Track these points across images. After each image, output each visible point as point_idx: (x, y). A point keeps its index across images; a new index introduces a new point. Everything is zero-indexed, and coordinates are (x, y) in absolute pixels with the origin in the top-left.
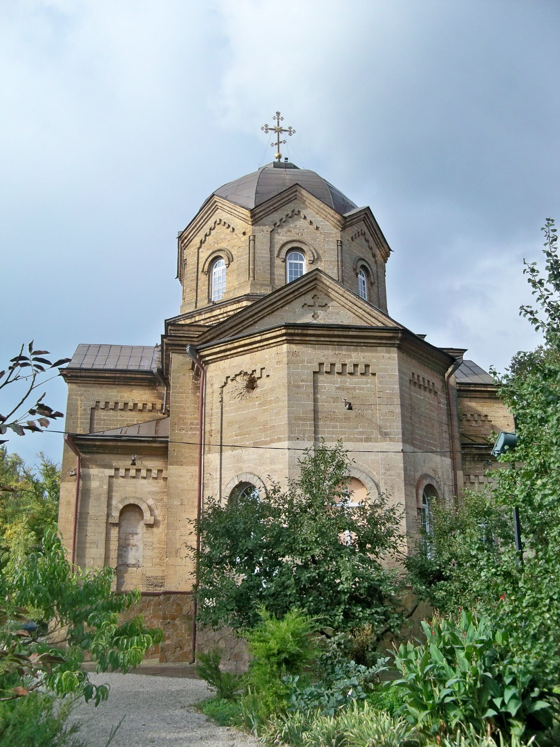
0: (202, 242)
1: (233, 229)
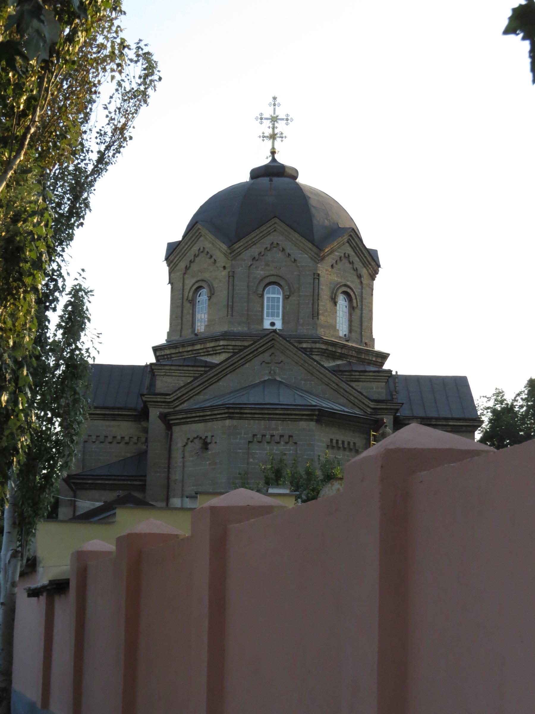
0: (187, 268)
1: (215, 260)
